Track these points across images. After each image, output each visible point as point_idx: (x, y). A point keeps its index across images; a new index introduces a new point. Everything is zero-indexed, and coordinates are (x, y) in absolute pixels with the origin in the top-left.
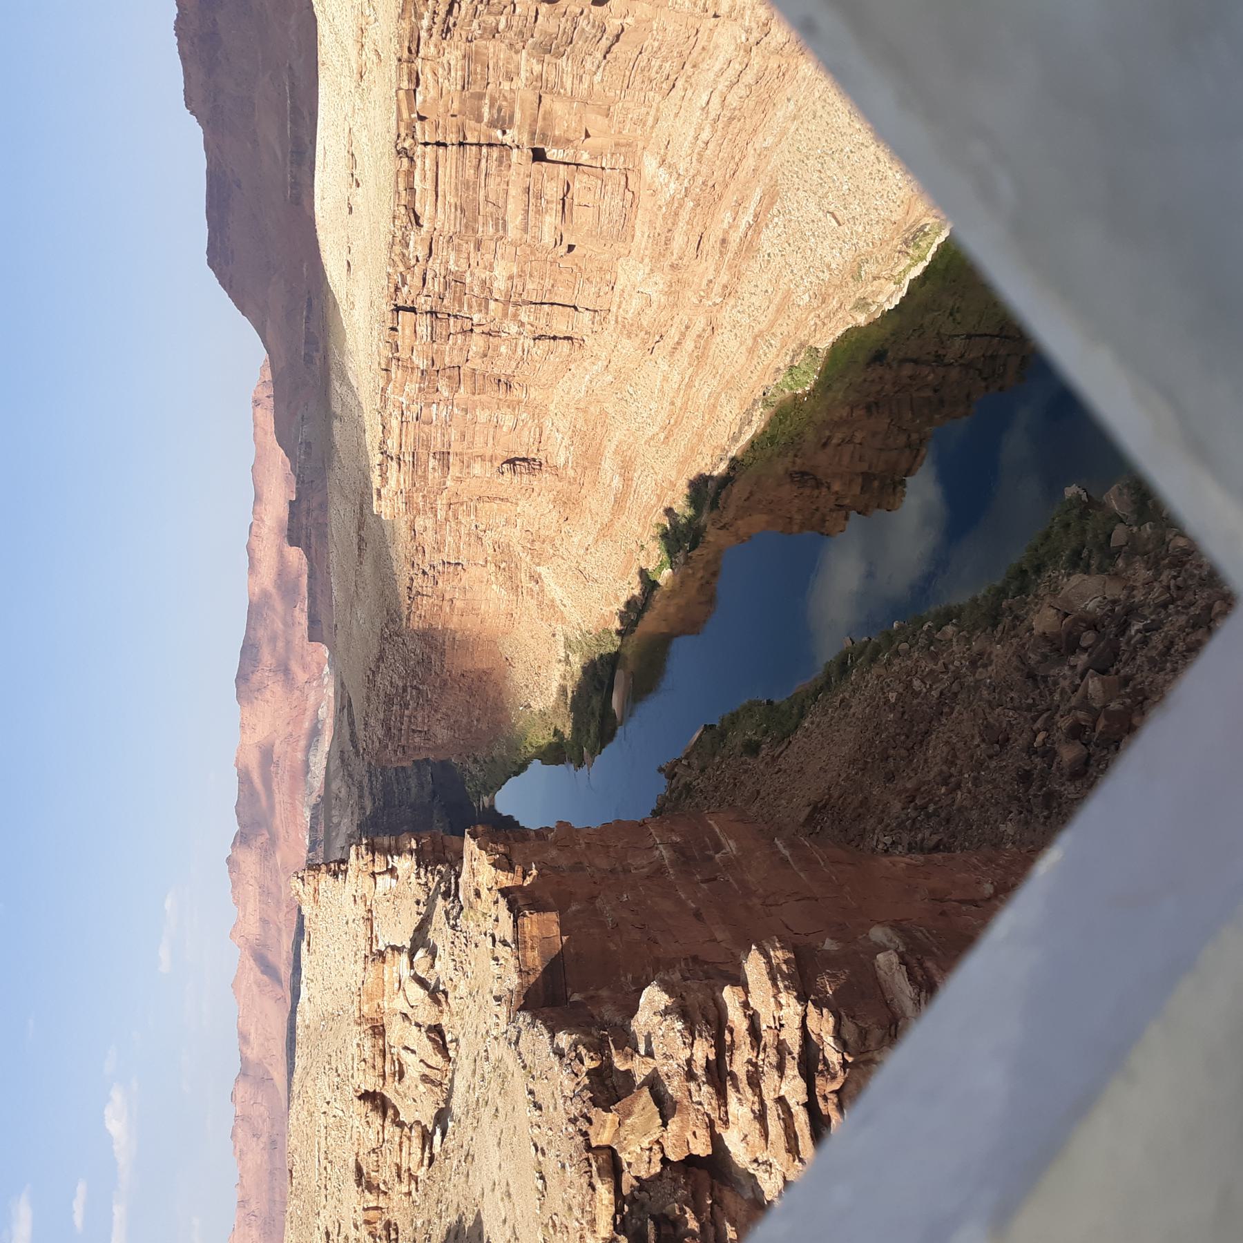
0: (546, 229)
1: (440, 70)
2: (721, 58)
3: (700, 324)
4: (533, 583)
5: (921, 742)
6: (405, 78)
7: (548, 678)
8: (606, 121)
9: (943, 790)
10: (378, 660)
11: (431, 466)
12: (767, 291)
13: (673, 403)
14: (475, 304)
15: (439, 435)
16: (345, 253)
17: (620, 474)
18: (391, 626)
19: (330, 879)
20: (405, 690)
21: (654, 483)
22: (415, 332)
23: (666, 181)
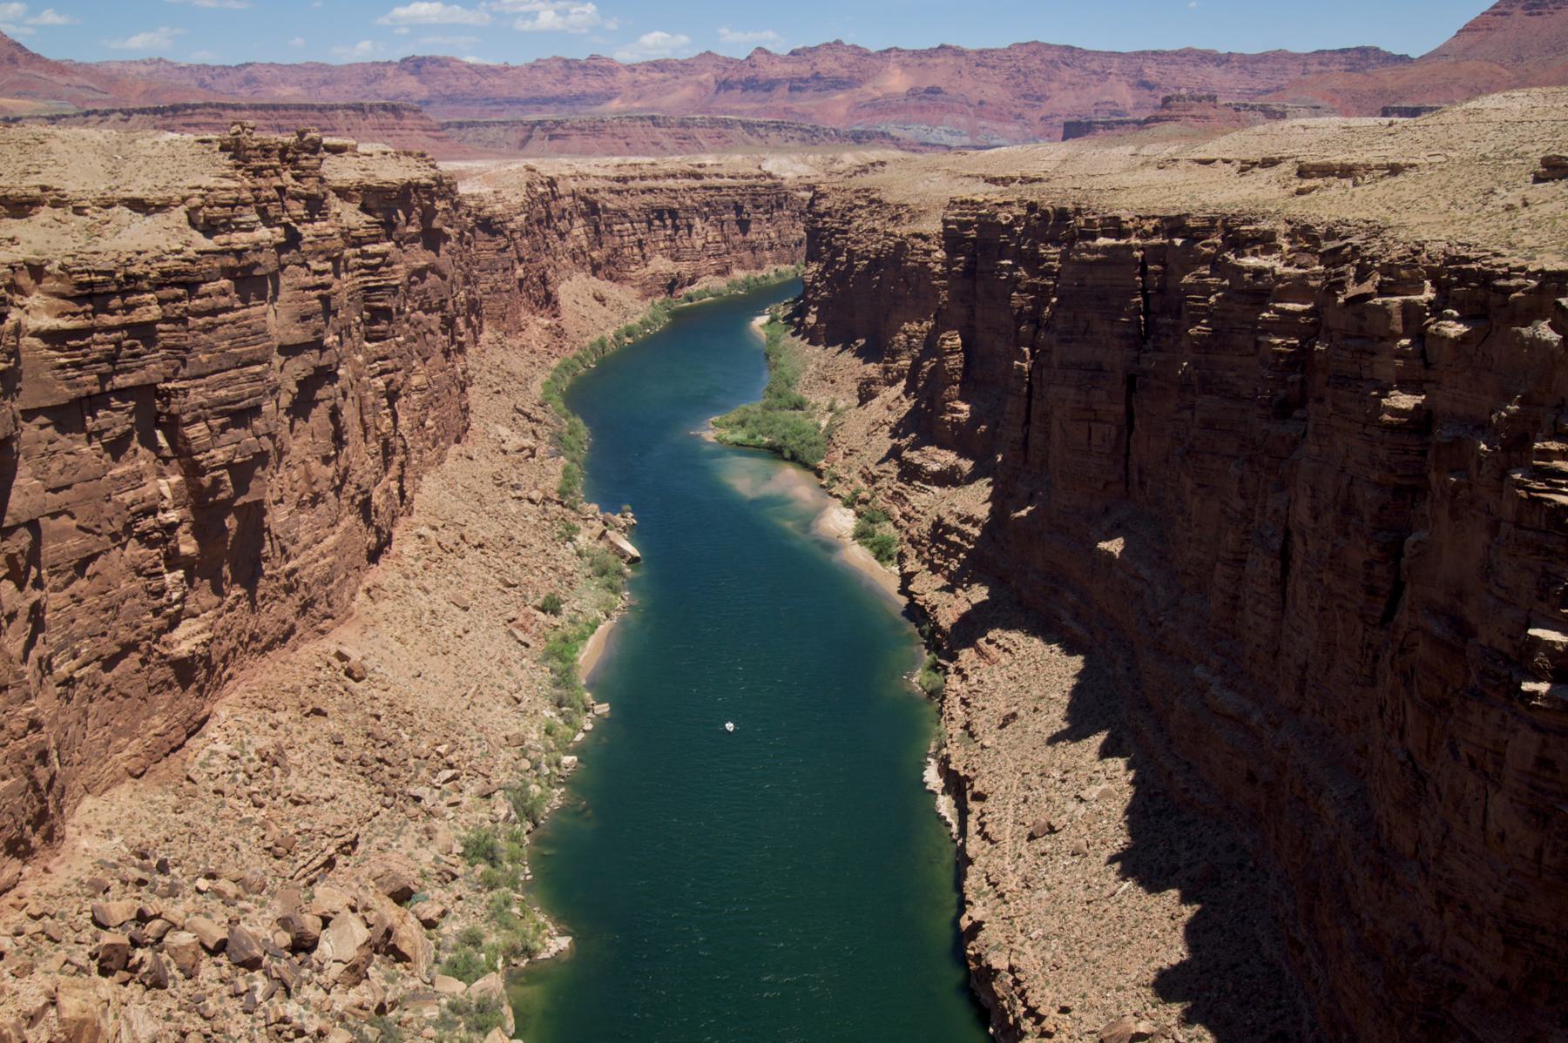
5: (363, 774)
10: (881, 201)
16: (1227, 156)
18: (908, 216)
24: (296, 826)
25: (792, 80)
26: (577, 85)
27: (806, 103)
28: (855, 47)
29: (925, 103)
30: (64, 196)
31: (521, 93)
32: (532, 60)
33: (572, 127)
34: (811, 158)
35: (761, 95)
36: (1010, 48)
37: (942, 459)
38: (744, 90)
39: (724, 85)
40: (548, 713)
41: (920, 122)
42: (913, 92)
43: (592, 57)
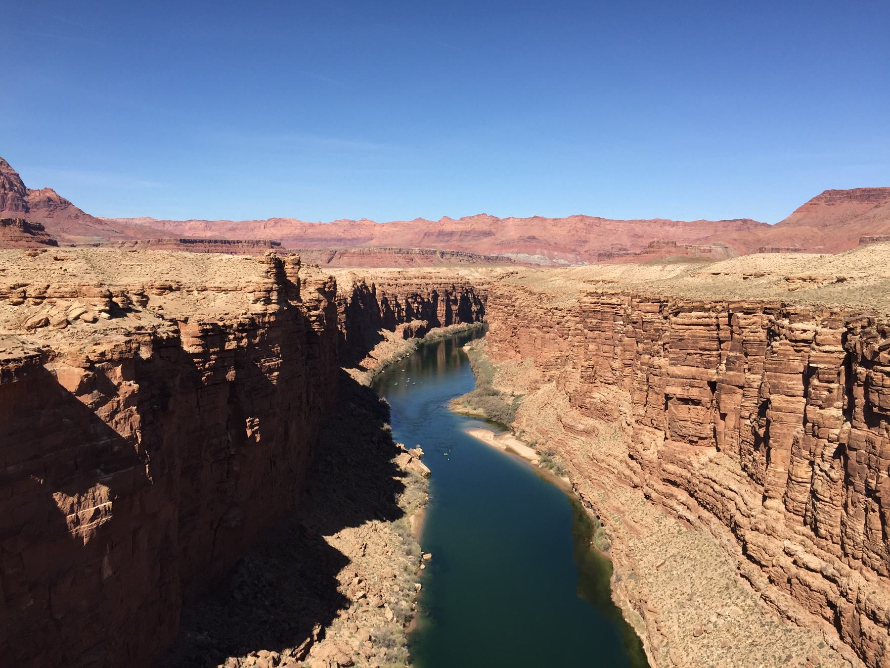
0: (674, 388)
1: (755, 327)
2: (749, 498)
3: (637, 480)
4: (549, 378)
6: (750, 306)
7: (505, 386)
8: (732, 427)
9: (267, 603)
10: (530, 292)
11: (593, 320)
12: (642, 520)
13: (603, 461)
14: (647, 346)
15: (609, 325)
17: (584, 429)
18: (546, 298)
19: (265, 269)
20: (513, 306)
21: (575, 448)
22: (649, 312)
23: (700, 462)
24: (289, 625)
26: (356, 233)
28: (492, 216)
30: (181, 285)
32: (333, 221)
34: (480, 270)
35: (446, 239)
36: (569, 218)
37: (585, 423)
40: (401, 559)
41: (525, 253)
42: (521, 239)
43: (363, 220)
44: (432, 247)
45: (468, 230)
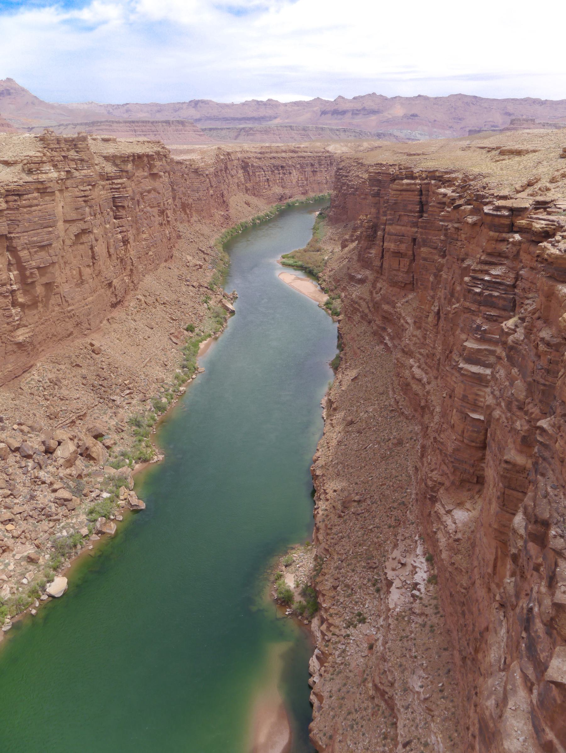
25: (353, 110)
26: (262, 112)
27: (358, 120)
28: (381, 96)
29: (410, 120)
31: (239, 116)
33: (257, 130)
35: (340, 117)
36: (448, 97)
38: (332, 114)
39: (324, 113)
42: (405, 116)
43: (269, 100)
44: (326, 124)
45: (359, 108)
